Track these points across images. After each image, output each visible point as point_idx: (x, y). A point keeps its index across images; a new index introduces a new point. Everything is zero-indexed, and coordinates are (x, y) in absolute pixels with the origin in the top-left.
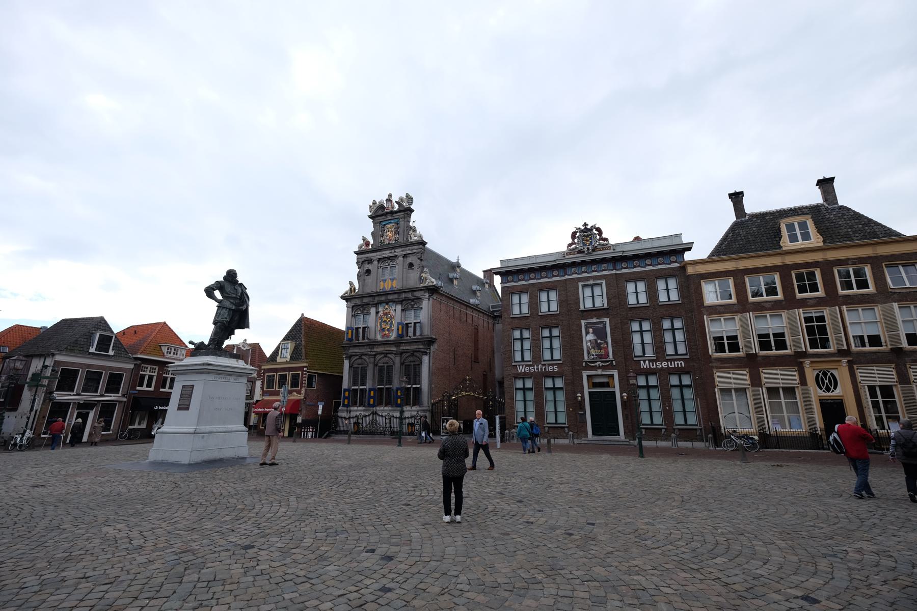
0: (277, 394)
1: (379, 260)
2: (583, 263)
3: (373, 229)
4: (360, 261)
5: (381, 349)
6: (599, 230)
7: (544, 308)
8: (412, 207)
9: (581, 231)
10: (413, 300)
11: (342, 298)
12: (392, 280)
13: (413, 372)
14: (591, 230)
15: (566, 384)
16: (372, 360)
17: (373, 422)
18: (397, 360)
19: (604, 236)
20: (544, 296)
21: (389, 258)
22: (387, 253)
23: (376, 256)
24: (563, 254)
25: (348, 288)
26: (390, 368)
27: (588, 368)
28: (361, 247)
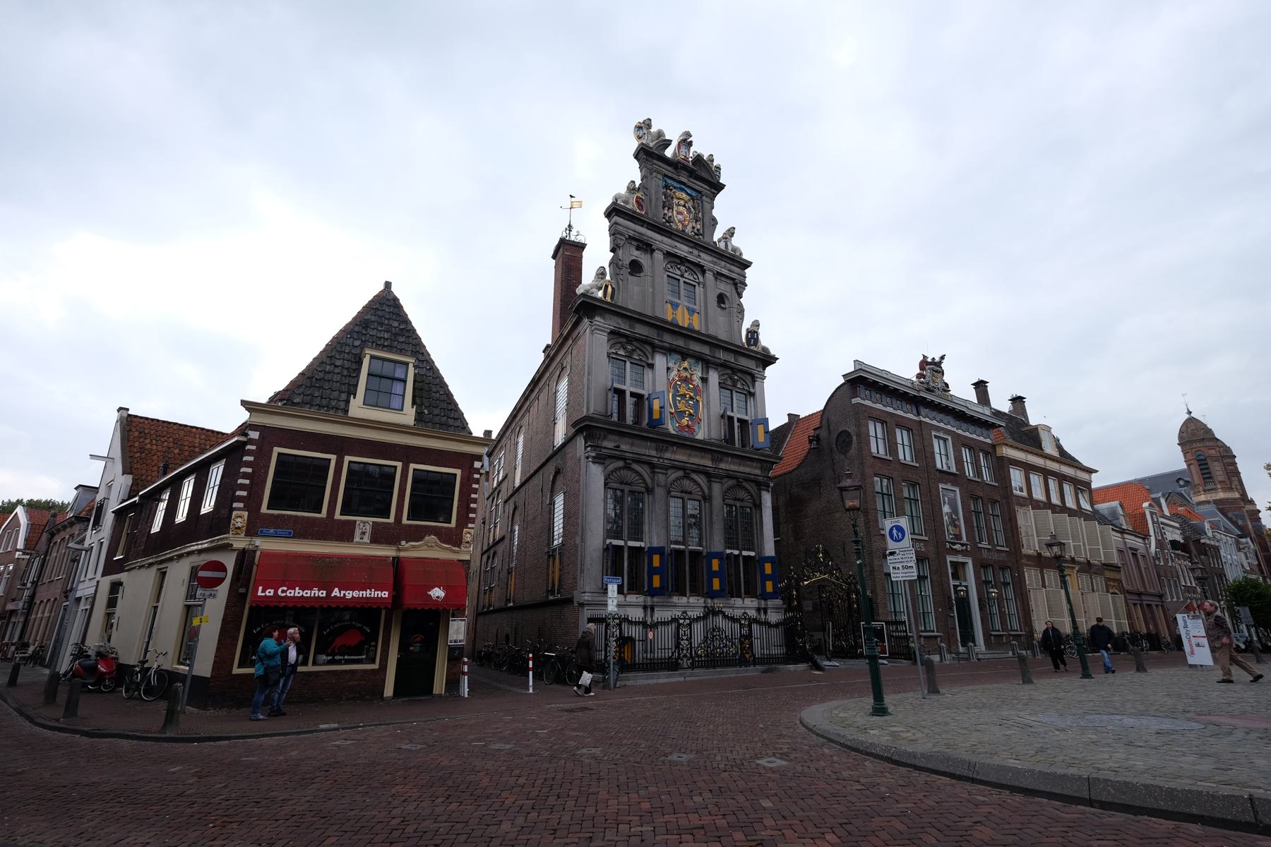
0: (345, 533)
1: (668, 254)
9: (930, 364)
10: (734, 370)
12: (691, 312)
17: (712, 635)
21: (683, 260)
22: (683, 250)
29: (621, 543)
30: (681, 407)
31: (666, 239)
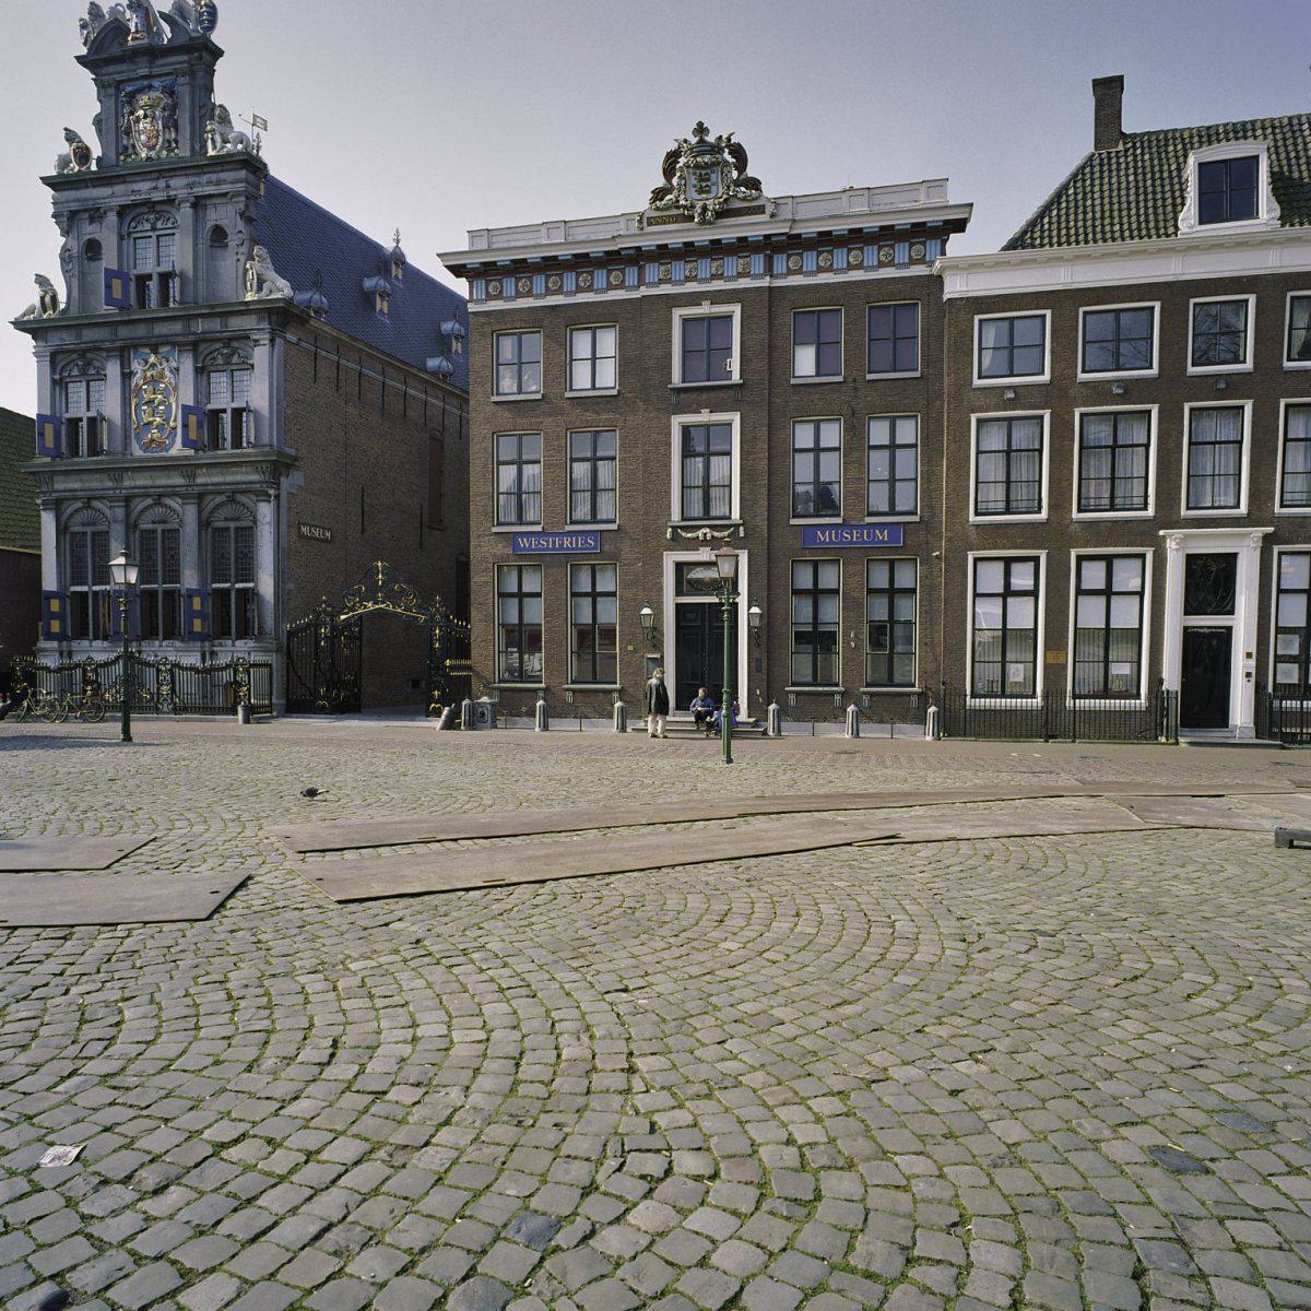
1: (122, 211)
2: (689, 251)
3: (97, 108)
4: (65, 209)
5: (142, 480)
6: (739, 153)
7: (581, 378)
8: (217, 37)
10: (227, 342)
11: (19, 325)
13: (229, 550)
14: (715, 149)
15: (625, 585)
16: (120, 512)
18: (190, 514)
19: (751, 172)
20: (582, 344)
23: (112, 196)
24: (644, 220)
25: (33, 297)
26: (172, 536)
27: (677, 542)
28: (63, 162)
29: (85, 588)
30: (146, 418)
31: (119, 189)
